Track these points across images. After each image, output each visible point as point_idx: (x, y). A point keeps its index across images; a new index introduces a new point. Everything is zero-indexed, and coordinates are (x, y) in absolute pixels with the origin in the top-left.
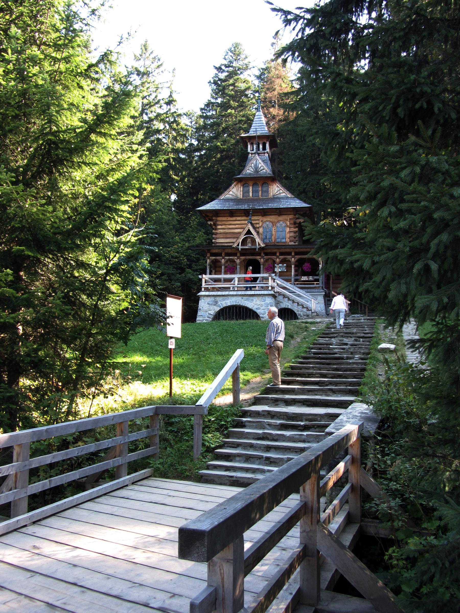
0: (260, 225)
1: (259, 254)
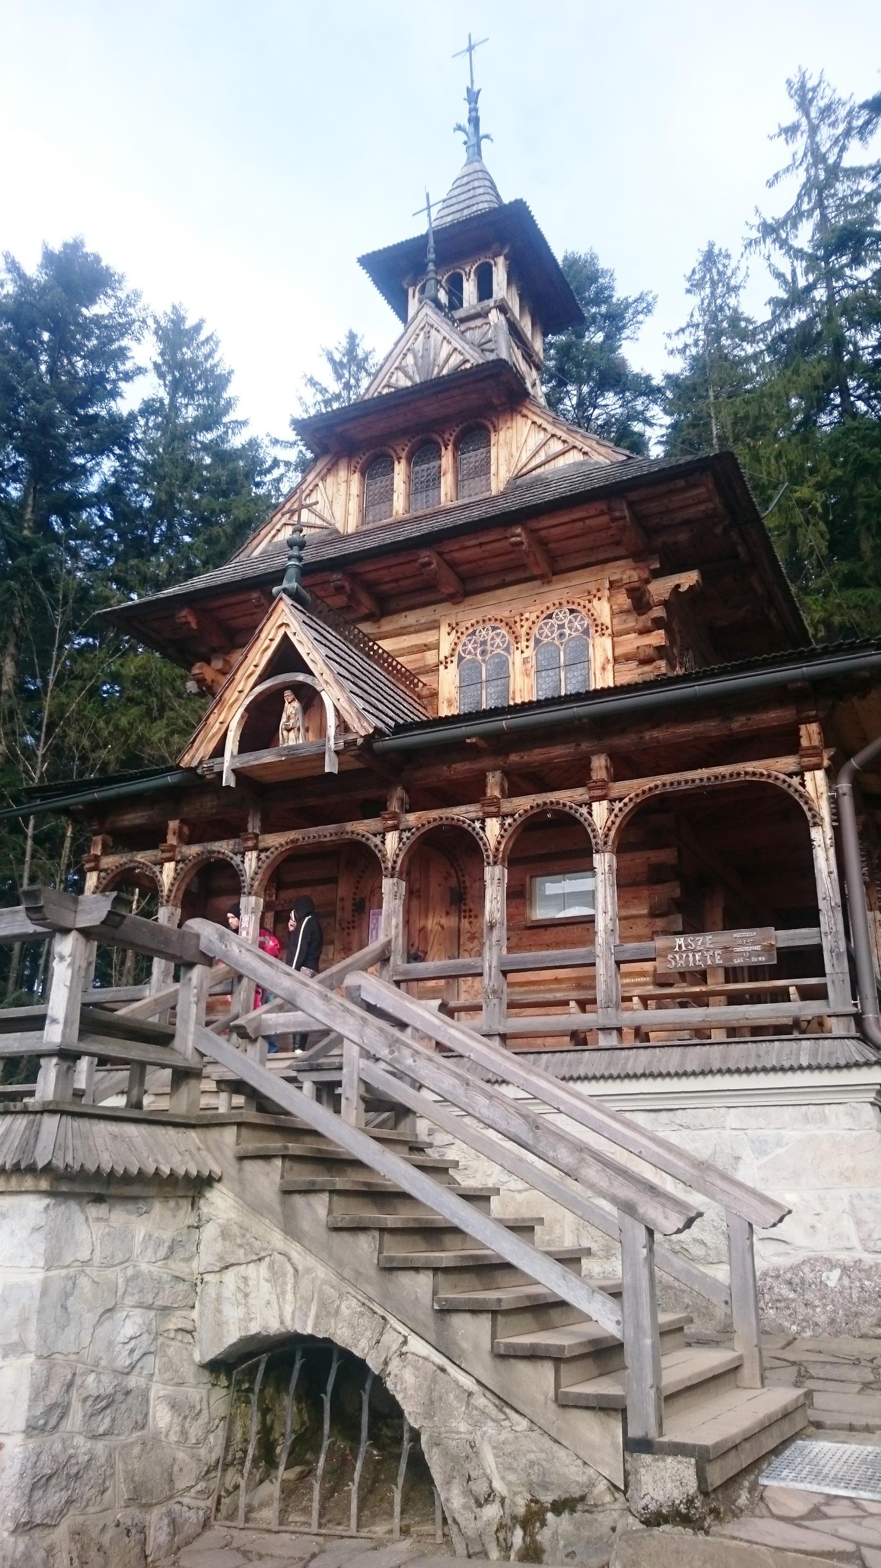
0: (445, 650)
1: (373, 808)
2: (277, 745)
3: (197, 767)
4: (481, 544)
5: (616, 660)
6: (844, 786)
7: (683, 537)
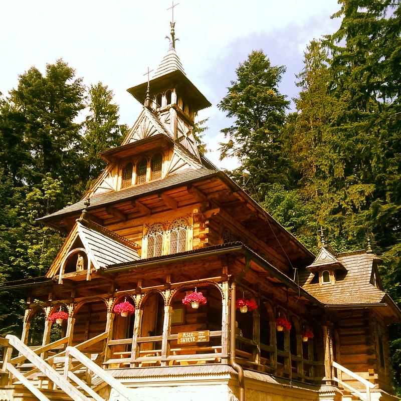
2: (76, 271)
3: (52, 278)
4: (152, 199)
5: (194, 238)
6: (233, 286)
7: (217, 196)
